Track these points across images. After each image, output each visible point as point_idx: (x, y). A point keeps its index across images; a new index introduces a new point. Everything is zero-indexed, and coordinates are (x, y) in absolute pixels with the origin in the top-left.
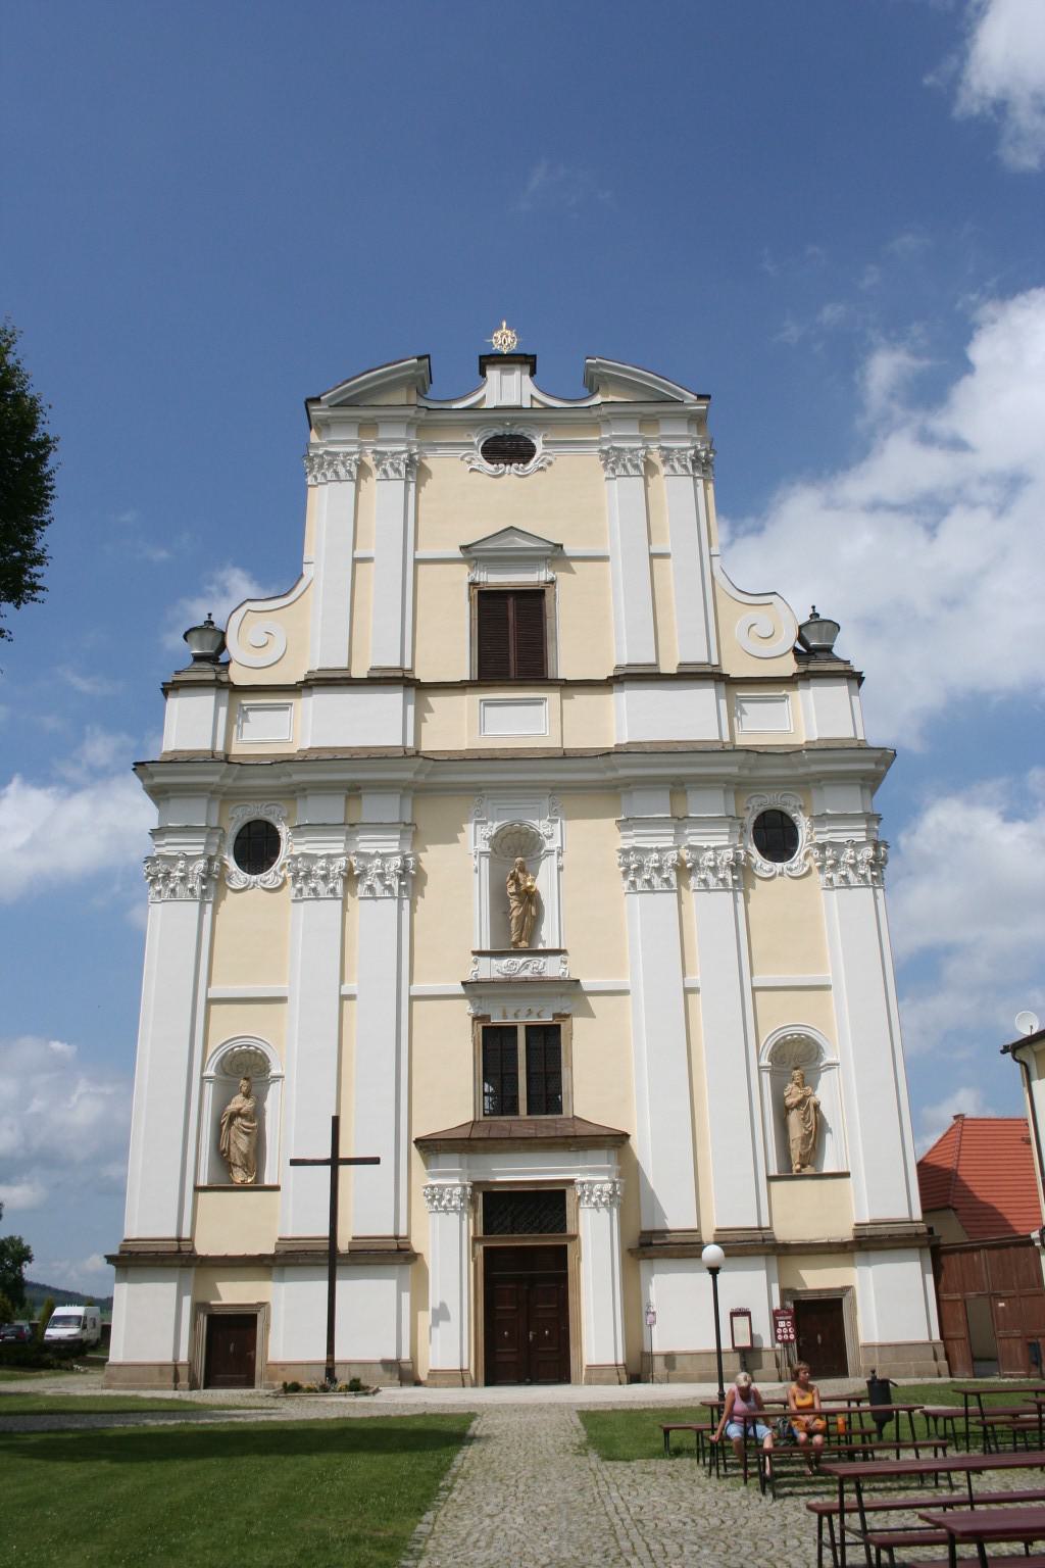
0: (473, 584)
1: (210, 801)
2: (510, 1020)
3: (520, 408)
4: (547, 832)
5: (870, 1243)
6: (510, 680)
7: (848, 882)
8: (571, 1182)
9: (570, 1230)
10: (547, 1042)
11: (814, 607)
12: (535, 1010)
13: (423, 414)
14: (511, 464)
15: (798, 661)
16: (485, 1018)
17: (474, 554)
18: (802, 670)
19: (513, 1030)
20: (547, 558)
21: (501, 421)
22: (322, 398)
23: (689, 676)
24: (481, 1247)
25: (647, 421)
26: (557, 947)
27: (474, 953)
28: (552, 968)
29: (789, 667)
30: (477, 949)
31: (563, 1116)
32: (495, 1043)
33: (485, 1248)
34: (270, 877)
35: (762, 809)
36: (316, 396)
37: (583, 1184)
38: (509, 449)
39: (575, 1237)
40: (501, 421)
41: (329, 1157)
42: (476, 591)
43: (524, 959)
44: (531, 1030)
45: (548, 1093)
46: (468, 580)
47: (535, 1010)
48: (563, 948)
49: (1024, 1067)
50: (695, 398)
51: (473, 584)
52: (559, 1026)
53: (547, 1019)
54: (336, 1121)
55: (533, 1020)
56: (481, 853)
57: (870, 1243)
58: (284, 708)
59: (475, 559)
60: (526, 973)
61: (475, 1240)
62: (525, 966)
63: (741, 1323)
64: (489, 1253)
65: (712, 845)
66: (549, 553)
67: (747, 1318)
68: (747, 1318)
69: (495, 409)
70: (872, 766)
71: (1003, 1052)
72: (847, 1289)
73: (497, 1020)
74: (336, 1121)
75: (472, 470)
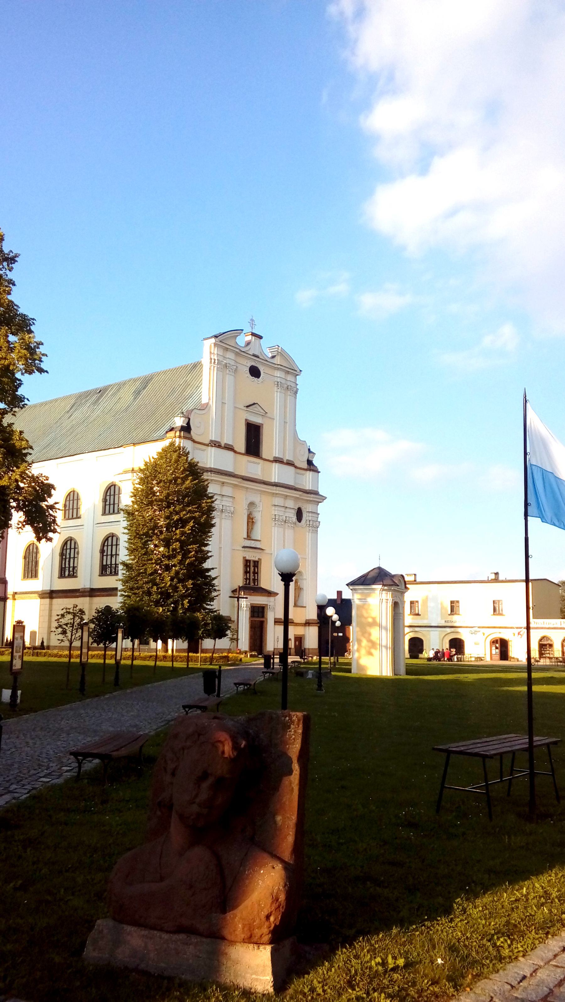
0: (246, 420)
3: (258, 357)
5: (308, 623)
8: (267, 605)
10: (256, 564)
13: (239, 352)
15: (308, 464)
16: (245, 557)
18: (309, 468)
19: (250, 561)
23: (290, 464)
26: (259, 539)
28: (257, 545)
29: (305, 466)
31: (259, 586)
32: (247, 563)
38: (255, 372)
39: (267, 619)
44: (254, 562)
45: (256, 580)
46: (245, 418)
51: (246, 420)
53: (257, 559)
55: (254, 559)
57: (308, 623)
58: (204, 450)
62: (254, 543)
69: (254, 355)
70: (320, 501)
72: (304, 635)
73: (247, 558)
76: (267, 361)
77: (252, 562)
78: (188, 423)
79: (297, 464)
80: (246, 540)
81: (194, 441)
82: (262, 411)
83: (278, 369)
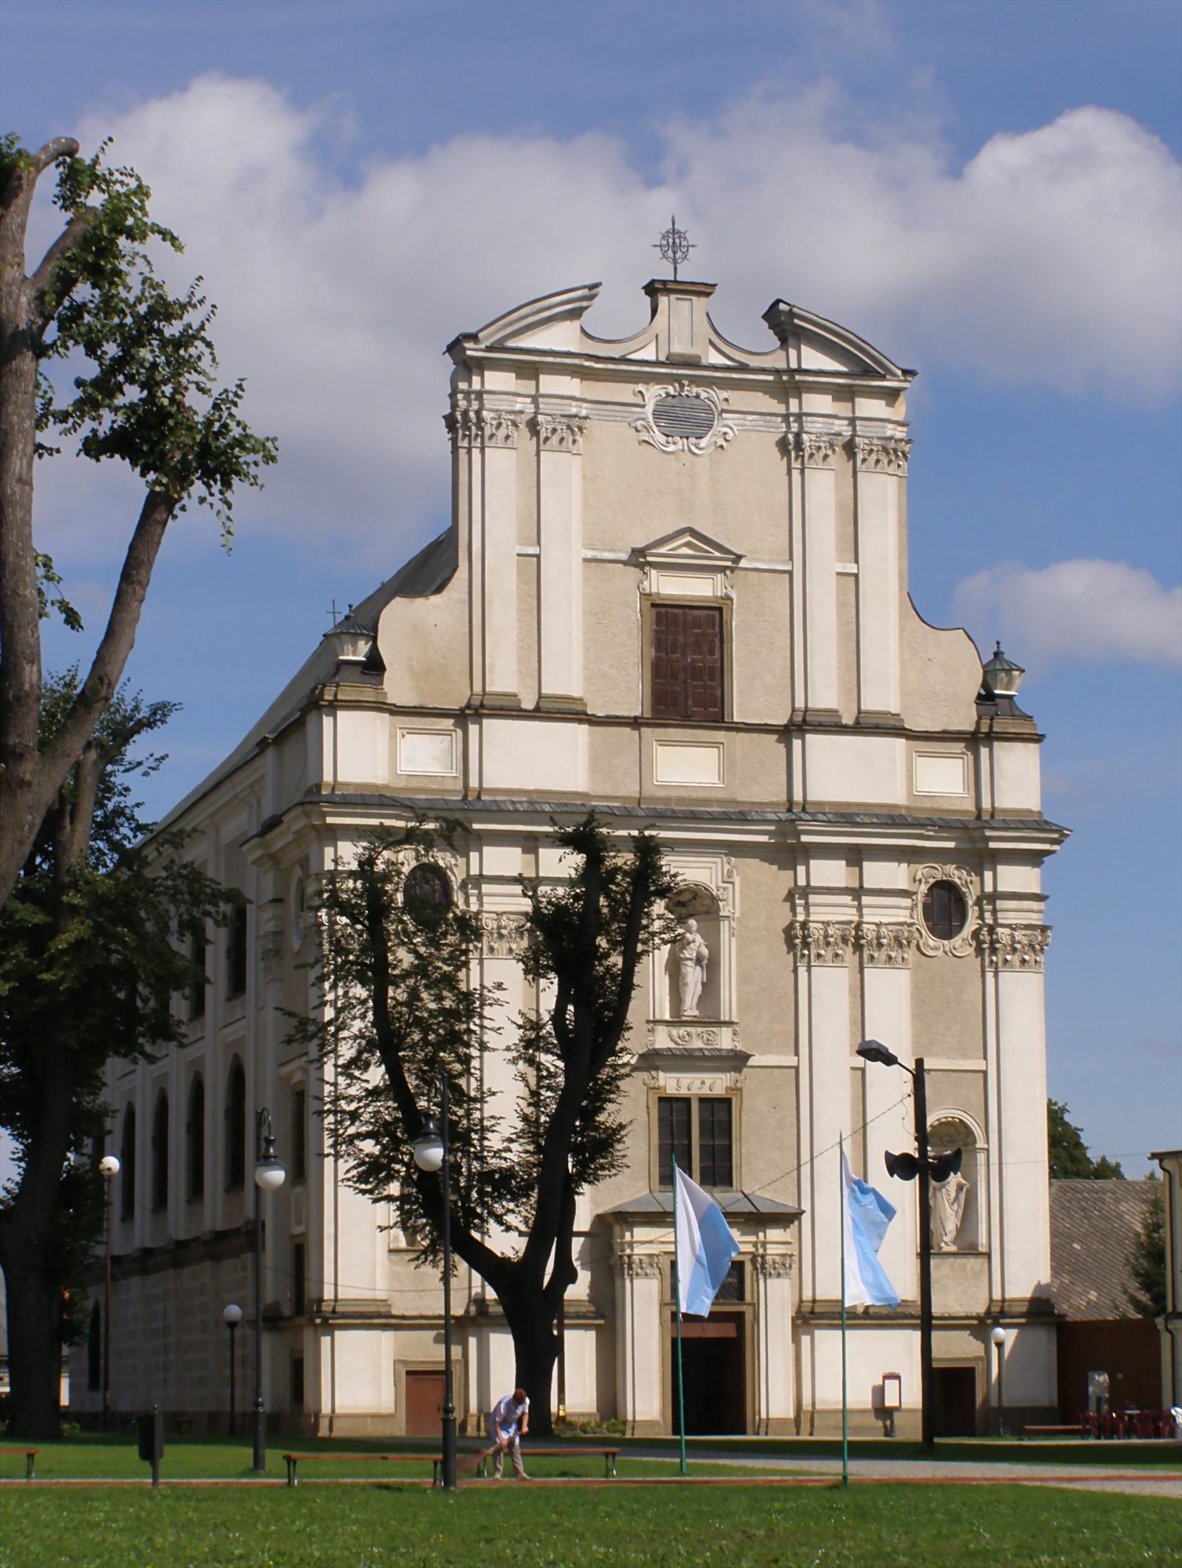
0: (645, 596)
2: (683, 1092)
6: (687, 717)
7: (1012, 966)
11: (998, 643)
12: (708, 1083)
14: (687, 438)
17: (649, 559)
19: (687, 1101)
20: (725, 568)
21: (677, 379)
22: (481, 335)
24: (669, 1313)
25: (846, 394)
27: (648, 1022)
28: (725, 1040)
35: (932, 881)
36: (472, 330)
39: (755, 1306)
40: (677, 379)
42: (649, 603)
43: (700, 1030)
44: (703, 1100)
47: (708, 1083)
48: (734, 1019)
49: (1167, 1174)
50: (899, 373)
53: (719, 1091)
55: (705, 1092)
59: (650, 564)
60: (697, 1044)
63: (891, 1386)
65: (885, 920)
66: (729, 564)
67: (897, 1381)
68: (897, 1381)
71: (1149, 1159)
73: (671, 1090)
75: (644, 441)
76: (743, 368)
78: (374, 651)
79: (912, 723)
80: (661, 1030)
81: (396, 711)
82: (718, 554)
83: (798, 390)
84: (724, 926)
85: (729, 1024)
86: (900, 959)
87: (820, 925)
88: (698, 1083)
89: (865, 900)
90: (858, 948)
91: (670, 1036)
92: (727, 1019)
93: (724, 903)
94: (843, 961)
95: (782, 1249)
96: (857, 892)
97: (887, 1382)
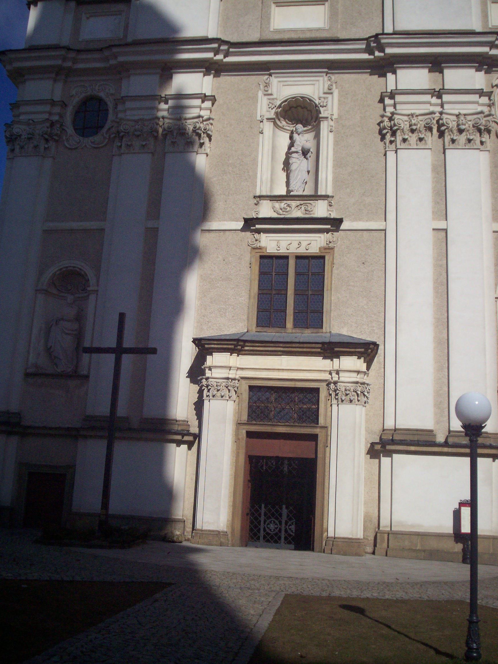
1: (55, 81)
2: (283, 251)
4: (322, 102)
9: (321, 421)
12: (304, 244)
19: (286, 258)
27: (255, 197)
30: (258, 194)
33: (248, 433)
34: (97, 138)
37: (335, 383)
41: (114, 345)
43: (298, 203)
44: (299, 257)
47: (304, 244)
52: (323, 258)
54: (122, 316)
55: (302, 251)
56: (267, 119)
61: (239, 424)
64: (250, 435)
74: (122, 316)
77: (292, 262)
84: (324, 126)
85: (325, 197)
86: (478, 142)
87: (406, 118)
88: (295, 245)
89: (445, 98)
90: (441, 134)
91: (273, 208)
92: (323, 193)
93: (324, 108)
94: (426, 144)
95: (354, 377)
96: (439, 94)
97: (462, 508)
